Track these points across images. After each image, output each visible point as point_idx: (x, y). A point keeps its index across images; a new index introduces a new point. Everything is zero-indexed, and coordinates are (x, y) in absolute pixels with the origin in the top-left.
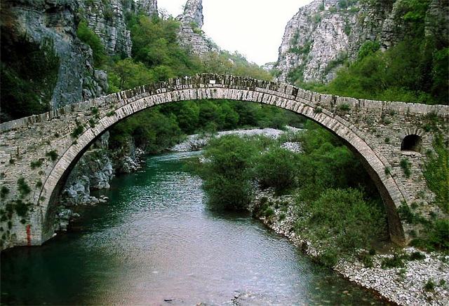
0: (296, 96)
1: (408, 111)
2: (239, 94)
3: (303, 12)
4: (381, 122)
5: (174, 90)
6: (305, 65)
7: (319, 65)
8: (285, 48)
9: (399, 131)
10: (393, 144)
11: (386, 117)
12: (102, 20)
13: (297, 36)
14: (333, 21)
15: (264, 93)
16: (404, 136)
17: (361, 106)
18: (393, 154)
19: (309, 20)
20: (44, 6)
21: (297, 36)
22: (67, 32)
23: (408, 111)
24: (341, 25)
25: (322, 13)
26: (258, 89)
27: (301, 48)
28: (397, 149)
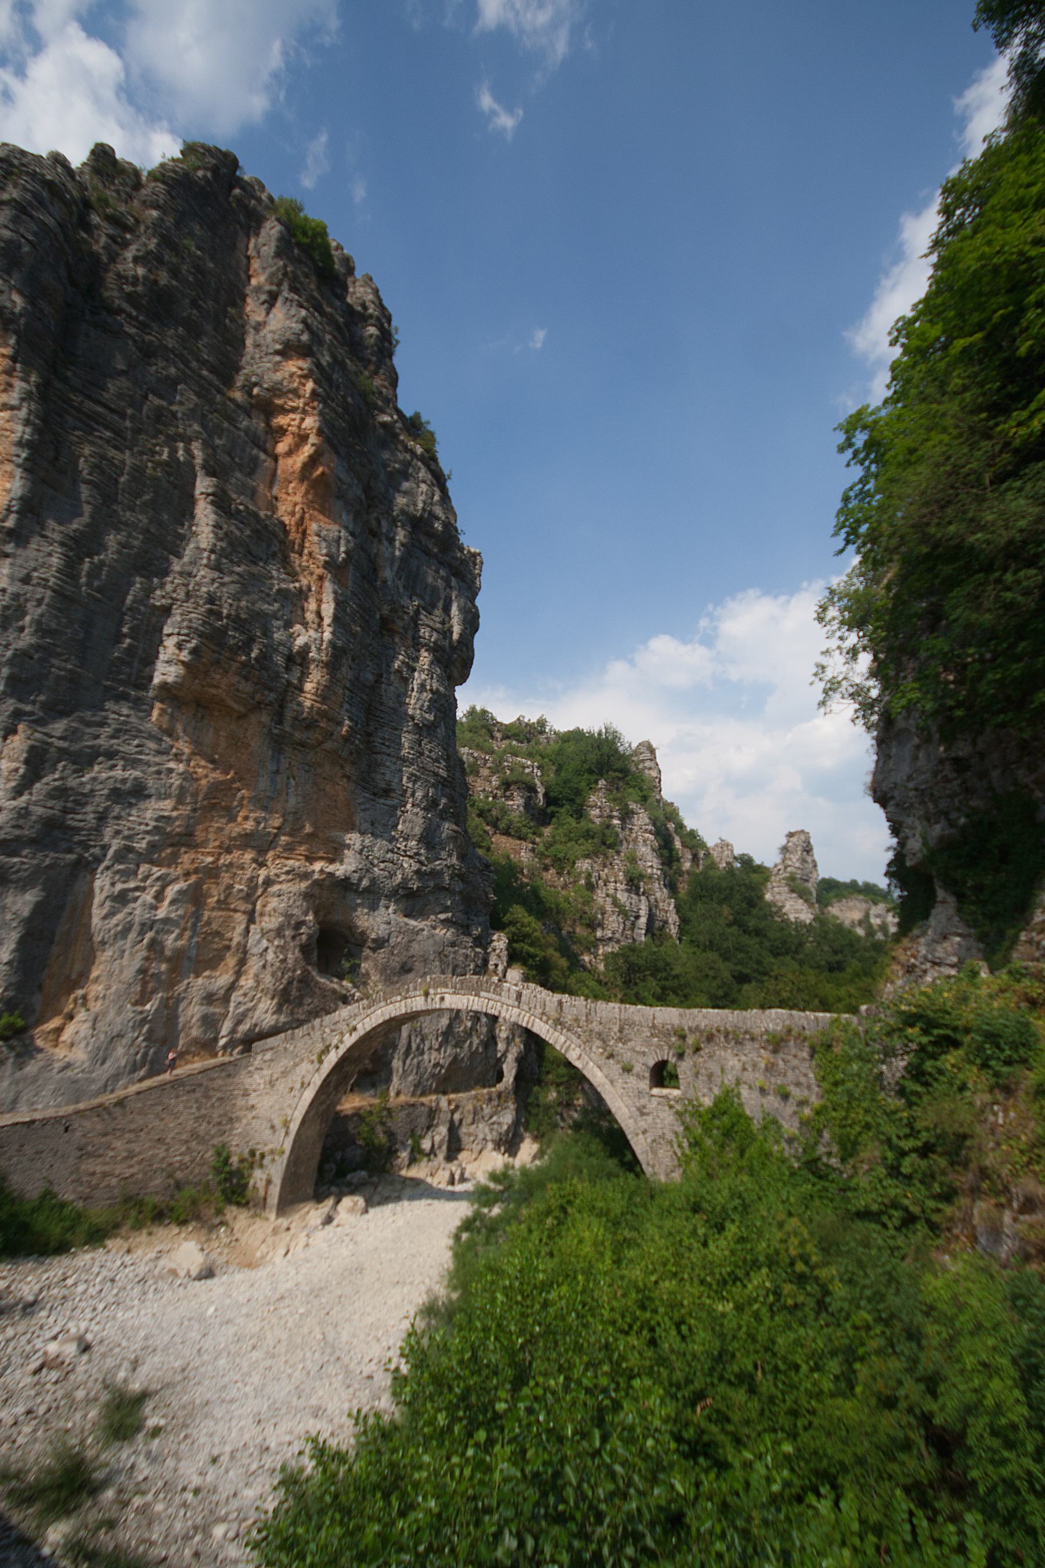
4: (620, 1039)
9: (644, 1053)
11: (625, 1032)
12: (623, 887)
18: (640, 1093)
26: (483, 994)
28: (644, 1085)
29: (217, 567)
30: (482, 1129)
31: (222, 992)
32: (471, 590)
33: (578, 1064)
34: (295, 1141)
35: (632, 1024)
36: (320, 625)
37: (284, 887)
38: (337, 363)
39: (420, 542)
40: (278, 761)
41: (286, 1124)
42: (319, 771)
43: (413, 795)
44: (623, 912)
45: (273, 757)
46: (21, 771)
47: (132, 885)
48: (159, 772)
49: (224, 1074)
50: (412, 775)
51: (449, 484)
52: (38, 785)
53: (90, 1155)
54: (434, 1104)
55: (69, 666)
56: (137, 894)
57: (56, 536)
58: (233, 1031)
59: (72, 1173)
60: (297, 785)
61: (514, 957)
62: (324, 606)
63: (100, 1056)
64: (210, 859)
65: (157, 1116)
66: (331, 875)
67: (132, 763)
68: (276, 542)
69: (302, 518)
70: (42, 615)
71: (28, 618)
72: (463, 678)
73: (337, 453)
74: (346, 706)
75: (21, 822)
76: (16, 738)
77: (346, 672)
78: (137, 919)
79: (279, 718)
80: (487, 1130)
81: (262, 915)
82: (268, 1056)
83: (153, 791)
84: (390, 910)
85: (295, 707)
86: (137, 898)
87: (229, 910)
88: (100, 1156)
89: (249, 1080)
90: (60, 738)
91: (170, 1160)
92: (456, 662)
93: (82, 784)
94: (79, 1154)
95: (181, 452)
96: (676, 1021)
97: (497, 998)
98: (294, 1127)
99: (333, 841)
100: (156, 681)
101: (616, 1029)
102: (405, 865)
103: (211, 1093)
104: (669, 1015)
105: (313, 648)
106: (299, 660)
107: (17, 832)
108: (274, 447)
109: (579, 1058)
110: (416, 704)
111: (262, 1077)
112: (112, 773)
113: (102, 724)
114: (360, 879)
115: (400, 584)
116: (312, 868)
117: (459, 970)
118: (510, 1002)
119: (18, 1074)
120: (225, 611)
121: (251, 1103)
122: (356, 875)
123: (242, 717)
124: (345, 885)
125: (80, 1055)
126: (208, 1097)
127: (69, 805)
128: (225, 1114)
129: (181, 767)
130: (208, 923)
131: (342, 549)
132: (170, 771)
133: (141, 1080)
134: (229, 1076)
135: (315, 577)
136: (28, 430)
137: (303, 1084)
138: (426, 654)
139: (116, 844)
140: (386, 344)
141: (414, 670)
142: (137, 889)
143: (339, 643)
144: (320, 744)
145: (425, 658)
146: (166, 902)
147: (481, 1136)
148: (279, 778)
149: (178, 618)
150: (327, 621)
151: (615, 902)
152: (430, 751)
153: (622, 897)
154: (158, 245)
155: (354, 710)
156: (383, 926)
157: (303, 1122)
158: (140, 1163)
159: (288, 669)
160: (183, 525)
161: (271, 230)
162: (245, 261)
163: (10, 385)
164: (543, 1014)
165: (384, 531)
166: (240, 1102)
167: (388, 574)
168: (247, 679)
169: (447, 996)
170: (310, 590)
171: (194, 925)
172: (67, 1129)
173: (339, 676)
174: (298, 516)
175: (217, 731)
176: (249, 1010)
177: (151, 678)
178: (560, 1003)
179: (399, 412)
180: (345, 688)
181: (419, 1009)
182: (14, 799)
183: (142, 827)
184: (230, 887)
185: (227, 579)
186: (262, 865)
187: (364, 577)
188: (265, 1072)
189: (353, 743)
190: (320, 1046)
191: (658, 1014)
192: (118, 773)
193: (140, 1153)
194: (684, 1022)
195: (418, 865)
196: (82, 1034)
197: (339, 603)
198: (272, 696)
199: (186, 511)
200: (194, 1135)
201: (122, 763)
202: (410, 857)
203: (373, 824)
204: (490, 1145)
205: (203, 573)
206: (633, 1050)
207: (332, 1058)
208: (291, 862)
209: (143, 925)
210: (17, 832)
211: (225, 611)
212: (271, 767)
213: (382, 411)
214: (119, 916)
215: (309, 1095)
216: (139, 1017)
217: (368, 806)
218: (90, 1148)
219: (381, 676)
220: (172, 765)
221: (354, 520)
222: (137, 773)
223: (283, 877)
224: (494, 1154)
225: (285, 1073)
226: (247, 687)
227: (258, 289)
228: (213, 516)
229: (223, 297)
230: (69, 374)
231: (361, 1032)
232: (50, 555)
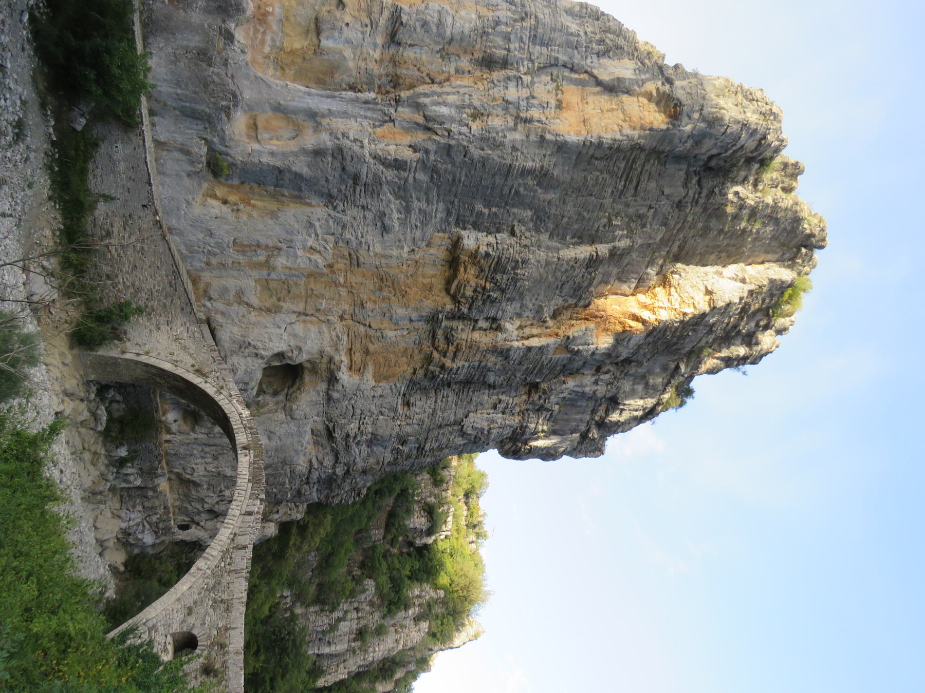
1: (234, 629)
2: (244, 472)
4: (215, 601)
9: (203, 624)
10: (183, 621)
11: (222, 606)
16: (195, 632)
20: (331, 421)
22: (311, 462)
23: (234, 629)
26: (250, 485)
28: (176, 628)
29: (548, 263)
30: (136, 516)
31: (246, 300)
32: (575, 452)
34: (132, 361)
35: (227, 610)
36: (523, 338)
37: (327, 335)
38: (711, 329)
39: (600, 405)
40: (419, 321)
41: (147, 353)
42: (416, 351)
43: (407, 424)
44: (333, 628)
45: (423, 316)
46: (389, 157)
47: (319, 231)
48: (400, 241)
49: (184, 306)
50: (423, 422)
51: (648, 423)
52: (381, 167)
53: (125, 223)
54: (159, 471)
55: (463, 179)
56: (313, 235)
57: (546, 164)
58: (217, 312)
59: (113, 212)
60: (403, 336)
61: (285, 528)
62: (536, 339)
63: (196, 223)
64: (342, 281)
65: (153, 263)
66: (339, 368)
67: (403, 223)
68: (575, 301)
69: (596, 317)
70: (493, 159)
71: (490, 152)
72: (505, 454)
73: (648, 335)
74: (467, 364)
75: (355, 159)
76: (411, 153)
77: (492, 360)
78: (295, 237)
79: (452, 317)
80: (138, 520)
81: (304, 321)
83: (386, 238)
84: (316, 418)
85: (460, 328)
86: (310, 236)
87: (307, 298)
88: (125, 229)
89: (179, 324)
90: (414, 178)
91: (120, 277)
92: (515, 446)
93: (385, 194)
94: (127, 215)
95: (620, 232)
96: (231, 648)
98: (144, 359)
99: (364, 368)
100: (463, 232)
101: (225, 597)
102: (352, 426)
103: (169, 299)
104: (237, 640)
105: (505, 336)
106: (495, 325)
107: (349, 158)
108: (640, 292)
109: (199, 569)
110: (478, 420)
111: (181, 332)
112: (395, 211)
113: (428, 201)
114: (338, 391)
115: (565, 394)
116: (343, 353)
117: (271, 479)
119: (184, 174)
120: (519, 271)
121: (162, 327)
122: (340, 388)
123: (447, 291)
124: (332, 380)
125: (197, 210)
126: (166, 297)
127: (370, 188)
128: (153, 310)
129: (405, 255)
130: (296, 284)
131: (581, 347)
132: (402, 248)
133: (179, 251)
134: (182, 309)
135: (557, 330)
136: (609, 141)
137: (177, 361)
138: (517, 421)
139: (347, 219)
140: (736, 363)
141: (503, 413)
142: (317, 235)
143: (511, 353)
144: (436, 349)
145: (515, 421)
146: (308, 255)
147: (133, 516)
148: (407, 322)
149: (508, 242)
150: (527, 343)
151: (339, 620)
152: (443, 434)
153: (344, 627)
154: (751, 206)
155: (465, 370)
156: (303, 413)
157: (147, 365)
158: (119, 255)
159: (487, 319)
160: (573, 237)
161: (785, 274)
162: (760, 260)
163: (634, 129)
165: (602, 377)
166: (162, 320)
167: (571, 383)
168: (475, 291)
169: (248, 458)
170: (546, 328)
171: (294, 276)
172: (144, 206)
173: (488, 356)
174: (597, 313)
175: (433, 276)
176: (233, 320)
177: (465, 229)
178: (245, 547)
179: (691, 378)
180: (480, 362)
181: (237, 438)
182: (371, 155)
183: (360, 235)
184: (322, 296)
185: (541, 270)
186: (342, 318)
187: (564, 366)
188: (185, 334)
189: (440, 373)
190: (206, 370)
191: (238, 631)
192: (395, 215)
193: (126, 255)
194: (231, 655)
195: (352, 435)
196: (212, 211)
197: (541, 349)
198: (465, 310)
199: (582, 238)
200: (139, 290)
201: (403, 216)
202: (359, 429)
203: (381, 396)
204: (124, 525)
205: (542, 255)
206: (206, 614)
207: (197, 380)
208: (345, 338)
209: (291, 241)
210: (349, 158)
211: (519, 271)
212: (414, 316)
213: (687, 366)
214: (296, 226)
215: (168, 366)
216: (225, 246)
217: (394, 391)
218: (130, 222)
219: (494, 388)
220: (406, 249)
221: (604, 354)
222: (397, 227)
223: (334, 334)
224: (117, 529)
225: (185, 348)
226: (469, 292)
227: (743, 270)
228: (582, 256)
229: (727, 248)
230: (652, 161)
231: (217, 398)
232: (534, 161)
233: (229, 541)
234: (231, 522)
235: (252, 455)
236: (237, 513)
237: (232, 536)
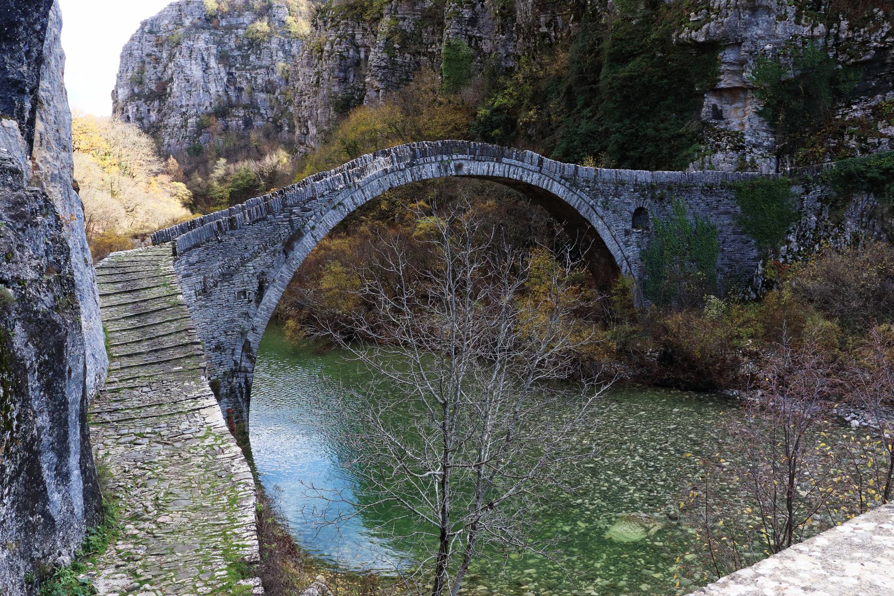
0: (541, 168)
1: (636, 180)
2: (485, 167)
3: (150, 28)
4: (615, 196)
5: (414, 165)
6: (162, 121)
7: (186, 120)
8: (123, 93)
9: (629, 204)
13: (142, 71)
14: (201, 44)
15: (510, 165)
17: (599, 177)
19: (159, 45)
21: (142, 71)
24: (215, 51)
25: (181, 30)
26: (505, 160)
27: (152, 92)
33: (586, 217)
82: (194, 258)
97: (521, 163)
104: (644, 175)
118: (533, 168)
164: (561, 177)
188: (193, 279)
190: (285, 232)
233: (568, 184)
234: (546, 182)
235: (460, 156)
236: (536, 176)
237: (563, 181)
